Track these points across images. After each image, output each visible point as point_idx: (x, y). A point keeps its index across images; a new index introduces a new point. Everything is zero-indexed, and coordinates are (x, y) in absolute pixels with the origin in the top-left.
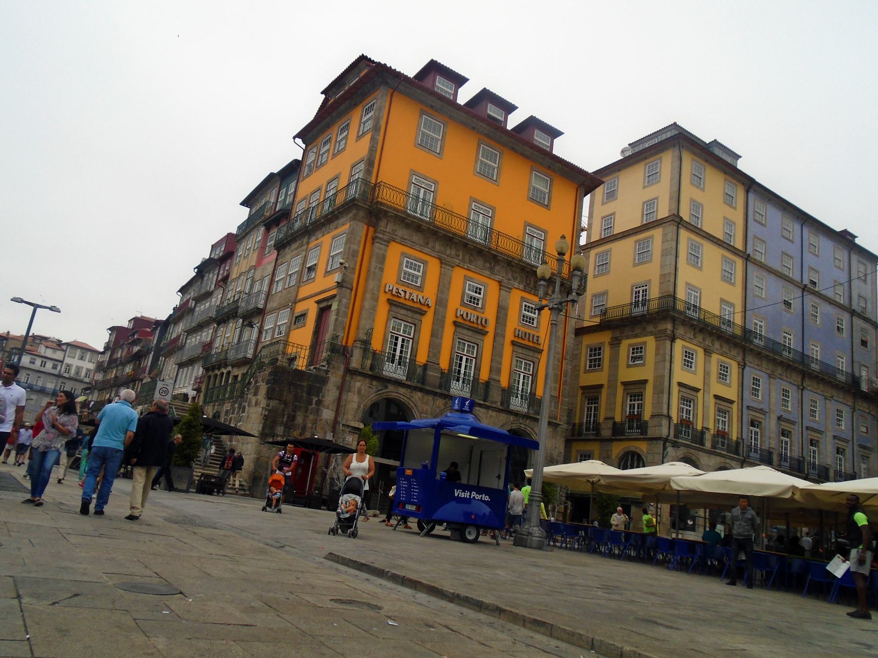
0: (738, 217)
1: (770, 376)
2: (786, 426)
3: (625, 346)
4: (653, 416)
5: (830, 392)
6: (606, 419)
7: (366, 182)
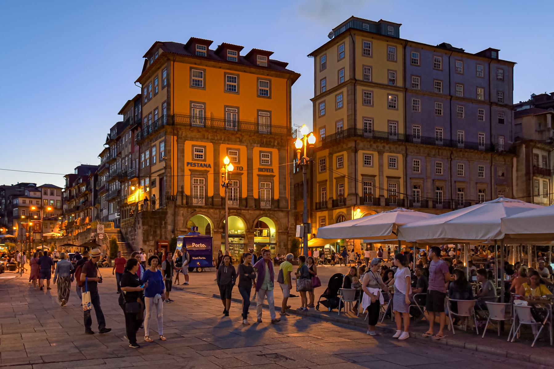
0: (398, 67)
2: (438, 184)
4: (348, 195)
6: (330, 198)
7: (168, 115)
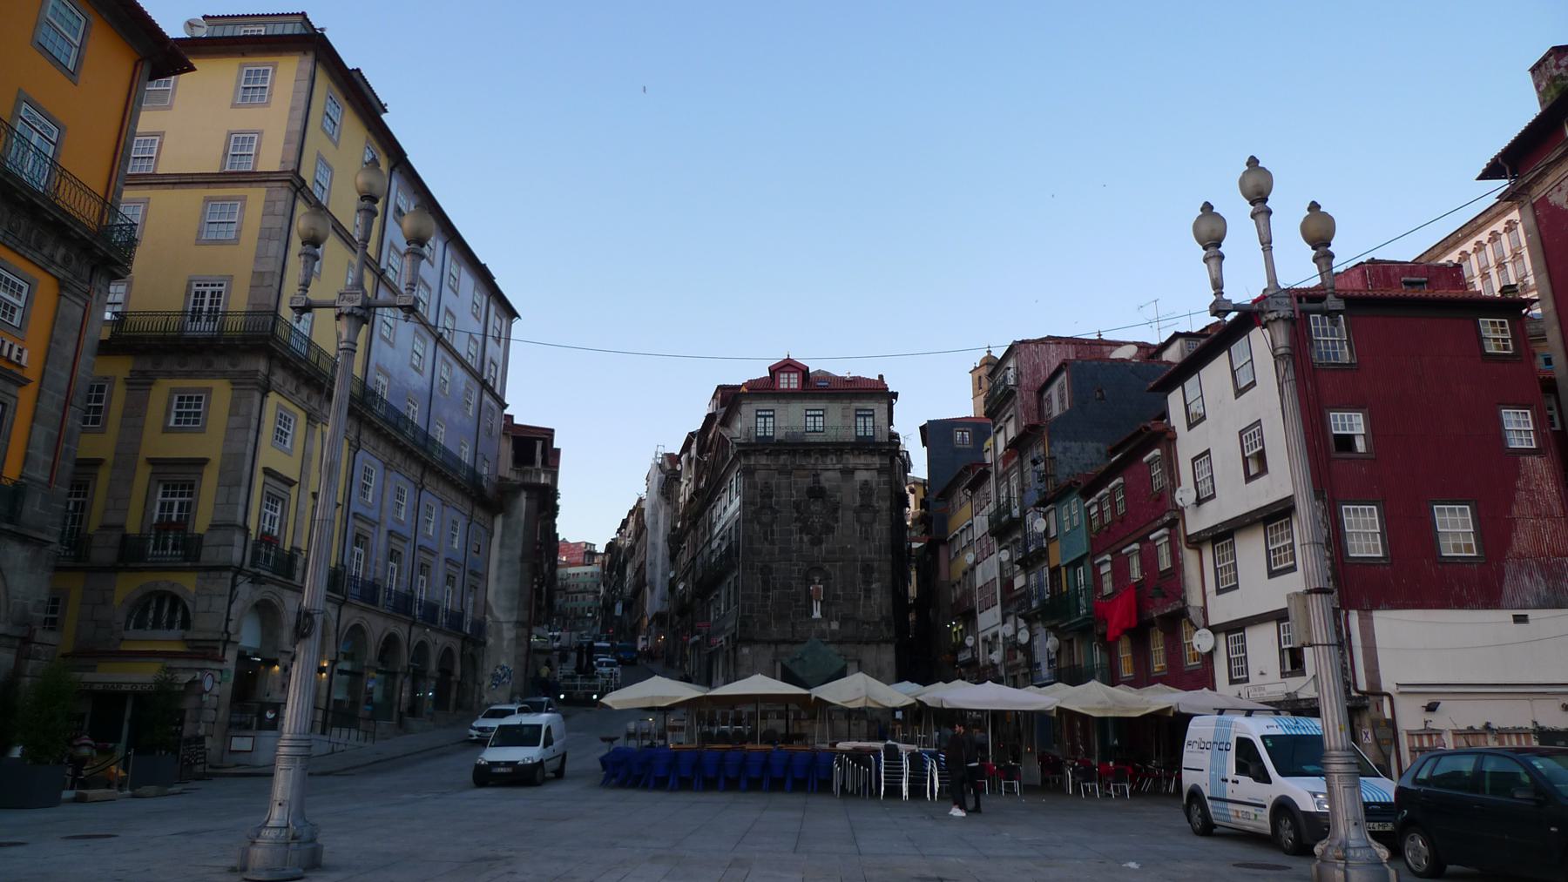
1: (386, 466)
3: (161, 393)
4: (214, 527)
5: (452, 495)
6: (104, 527)
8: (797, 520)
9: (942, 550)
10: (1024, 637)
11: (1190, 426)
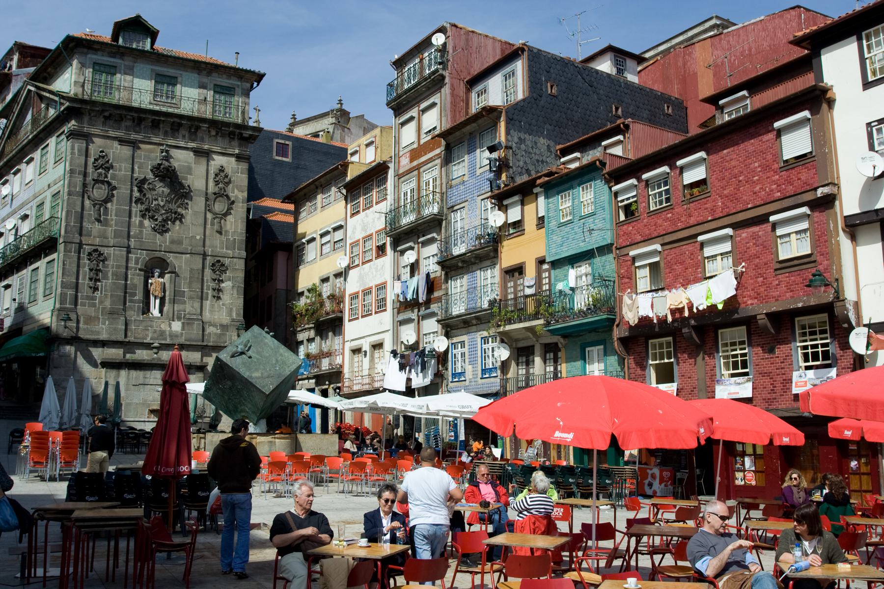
8: (138, 201)
9: (281, 259)
10: (441, 344)
11: (867, 85)
